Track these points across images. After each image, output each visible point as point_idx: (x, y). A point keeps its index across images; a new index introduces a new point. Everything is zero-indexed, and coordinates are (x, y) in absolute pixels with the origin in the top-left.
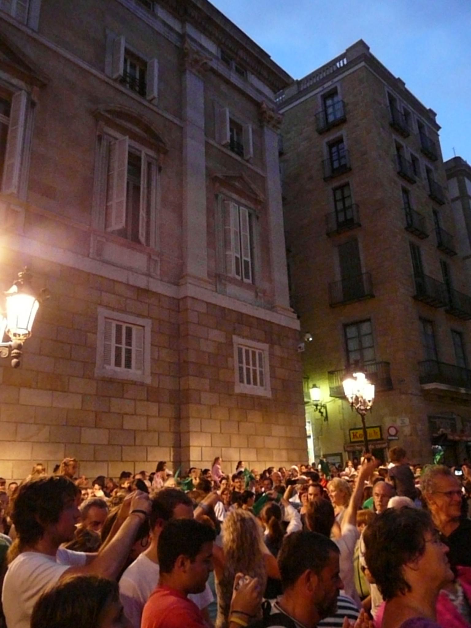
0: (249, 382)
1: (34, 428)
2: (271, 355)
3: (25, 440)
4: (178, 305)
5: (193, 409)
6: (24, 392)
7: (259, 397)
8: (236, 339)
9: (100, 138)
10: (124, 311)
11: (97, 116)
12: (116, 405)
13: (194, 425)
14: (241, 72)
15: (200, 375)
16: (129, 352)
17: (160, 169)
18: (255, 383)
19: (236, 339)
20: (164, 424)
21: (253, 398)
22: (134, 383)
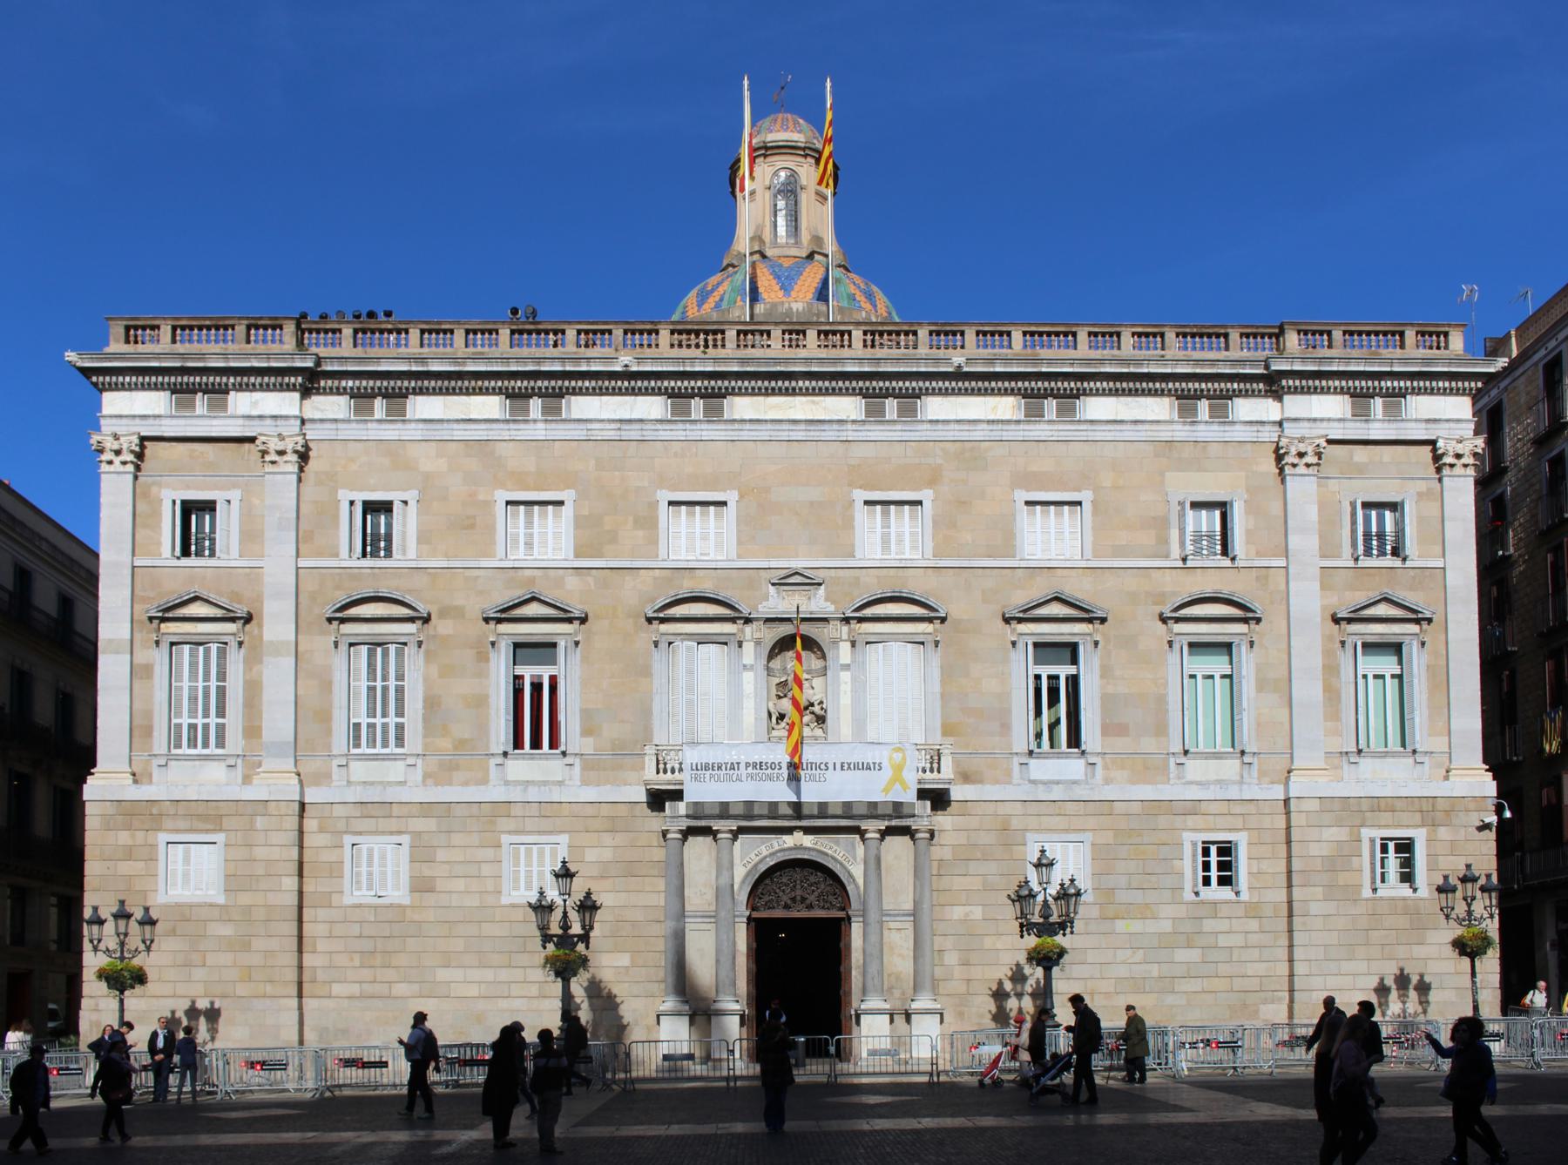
7: (1404, 899)
9: (1170, 643)
11: (1164, 620)
12: (1209, 925)
14: (1393, 413)
17: (1252, 644)
19: (1366, 833)
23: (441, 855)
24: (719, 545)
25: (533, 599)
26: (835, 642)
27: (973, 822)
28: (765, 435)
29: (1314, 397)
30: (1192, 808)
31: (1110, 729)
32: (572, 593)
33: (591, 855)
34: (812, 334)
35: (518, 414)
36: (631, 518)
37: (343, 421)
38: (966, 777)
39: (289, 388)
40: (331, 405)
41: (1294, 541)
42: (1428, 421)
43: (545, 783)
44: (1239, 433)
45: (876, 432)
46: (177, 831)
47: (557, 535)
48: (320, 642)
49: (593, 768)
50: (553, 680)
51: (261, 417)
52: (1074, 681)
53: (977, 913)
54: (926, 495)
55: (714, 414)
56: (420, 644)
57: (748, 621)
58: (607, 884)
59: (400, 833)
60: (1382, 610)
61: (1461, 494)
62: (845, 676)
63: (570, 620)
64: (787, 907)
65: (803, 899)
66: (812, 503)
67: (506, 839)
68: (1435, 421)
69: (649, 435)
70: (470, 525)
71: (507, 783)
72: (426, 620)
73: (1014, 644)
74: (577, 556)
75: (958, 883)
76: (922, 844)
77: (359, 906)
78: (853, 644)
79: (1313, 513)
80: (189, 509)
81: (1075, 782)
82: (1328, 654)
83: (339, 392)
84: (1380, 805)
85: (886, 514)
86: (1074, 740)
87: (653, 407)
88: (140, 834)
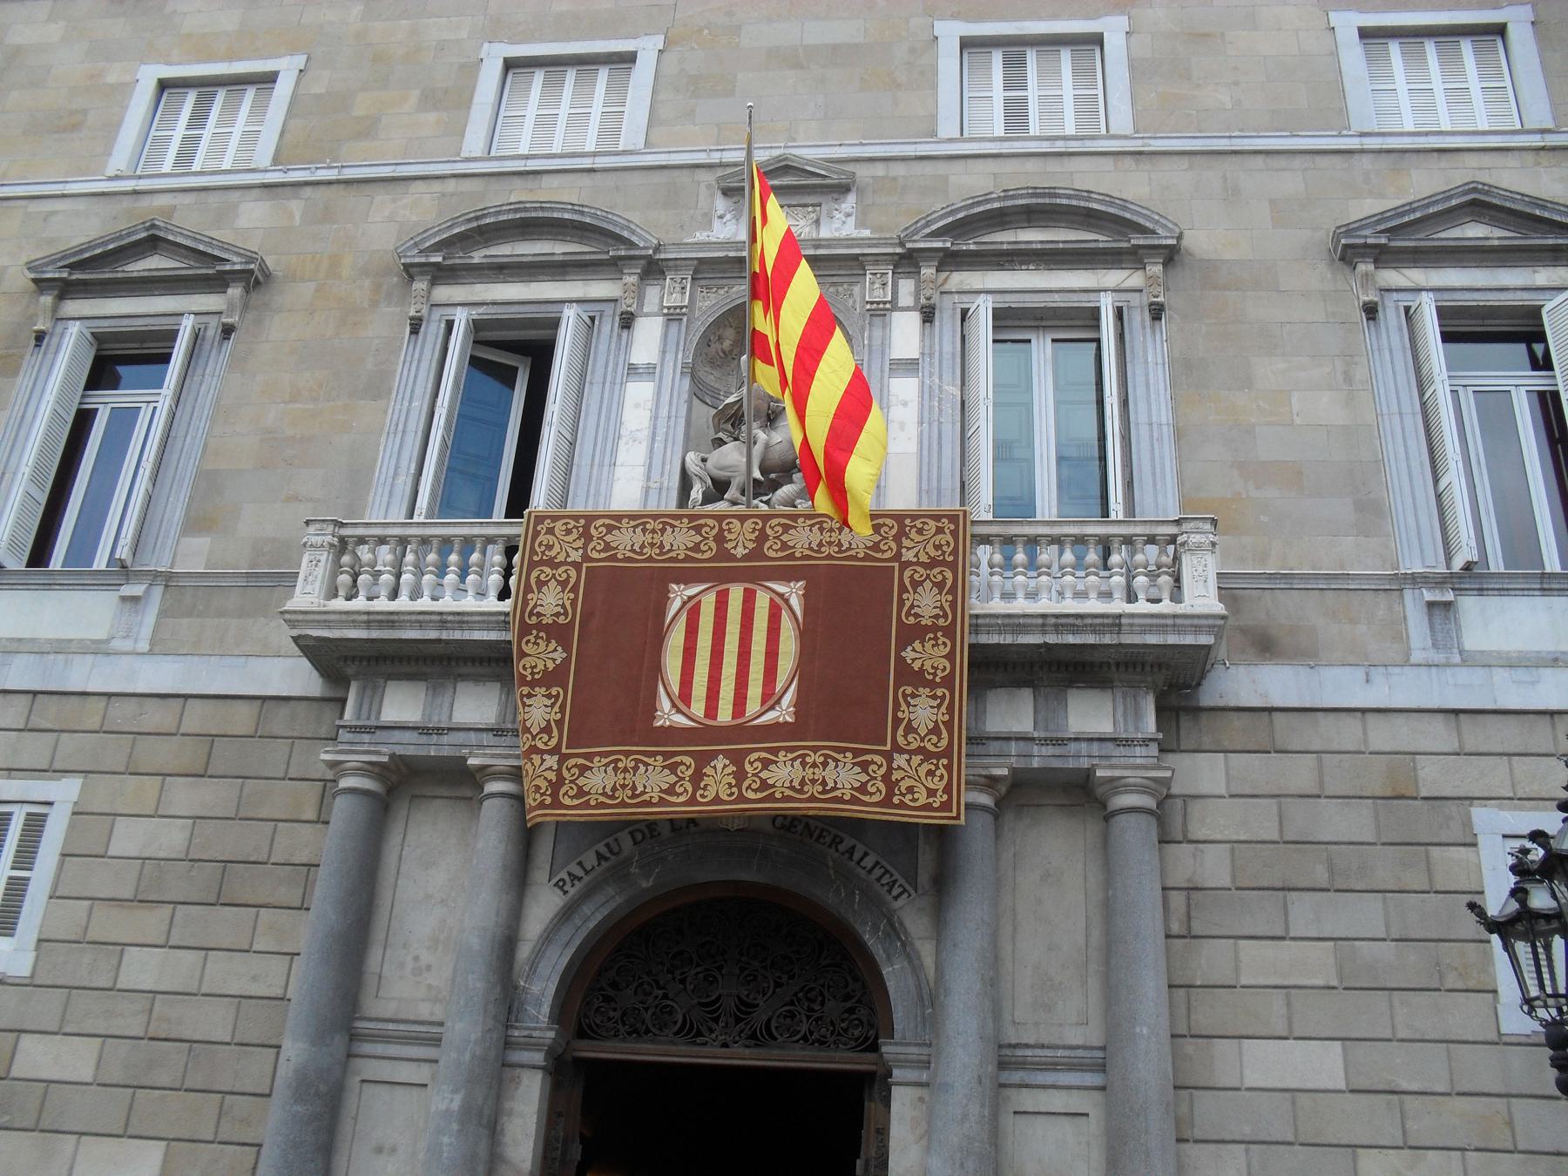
24: (611, 127)
25: (153, 243)
26: (881, 312)
27: (1298, 774)
32: (248, 228)
36: (415, 95)
38: (1265, 646)
43: (62, 647)
47: (250, 138)
53: (1322, 1065)
57: (653, 269)
58: (152, 922)
63: (218, 283)
64: (691, 1032)
65: (746, 1006)
66: (835, 48)
74: (276, 160)
75: (1260, 962)
76: (1135, 835)
78: (928, 315)
85: (1015, 65)
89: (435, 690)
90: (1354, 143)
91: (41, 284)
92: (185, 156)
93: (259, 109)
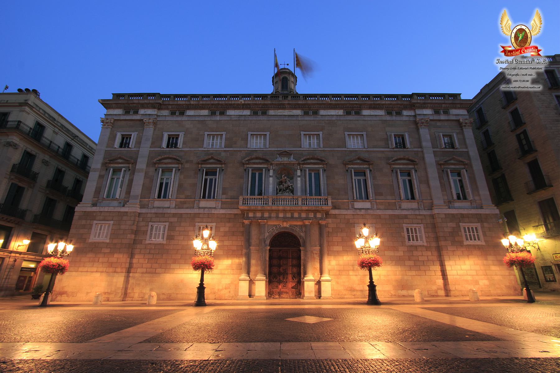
0: (471, 239)
1: (390, 262)
2: (482, 227)
3: (389, 265)
4: (432, 216)
5: (444, 252)
6: (386, 252)
8: (460, 224)
9: (392, 171)
10: (413, 223)
11: (390, 164)
12: (415, 253)
13: (446, 258)
14: (446, 112)
15: (446, 240)
16: (416, 236)
17: (416, 171)
18: (475, 239)
20: (435, 258)
21: (478, 245)
22: (420, 246)
23: (177, 229)
24: (265, 145)
25: (212, 158)
28: (277, 119)
29: (424, 110)
30: (406, 217)
31: (378, 194)
33: (222, 229)
34: (290, 98)
35: (213, 113)
37: (168, 116)
38: (335, 207)
39: (154, 108)
40: (166, 112)
41: (424, 144)
42: (456, 115)
43: (210, 208)
44: (405, 118)
45: (307, 118)
46: (99, 220)
48: (152, 169)
49: (224, 205)
50: (216, 179)
51: (146, 115)
52: (365, 181)
54: (321, 133)
55: (264, 113)
56: (179, 170)
57: (272, 164)
59: (166, 222)
60: (452, 162)
61: (469, 133)
62: (299, 179)
67: (197, 224)
68: (458, 115)
69: (247, 119)
70: (199, 140)
71: (199, 208)
72: (182, 164)
73: (347, 170)
75: (335, 239)
77: (151, 244)
78: (301, 170)
79: (428, 137)
80: (123, 137)
81: (368, 209)
82: (438, 173)
83: (167, 109)
84: (463, 216)
86: (367, 198)
87: (247, 112)
88: (89, 221)
89: (254, 213)
90: (346, 149)
91: (198, 164)
92: (213, 145)
93: (221, 139)
